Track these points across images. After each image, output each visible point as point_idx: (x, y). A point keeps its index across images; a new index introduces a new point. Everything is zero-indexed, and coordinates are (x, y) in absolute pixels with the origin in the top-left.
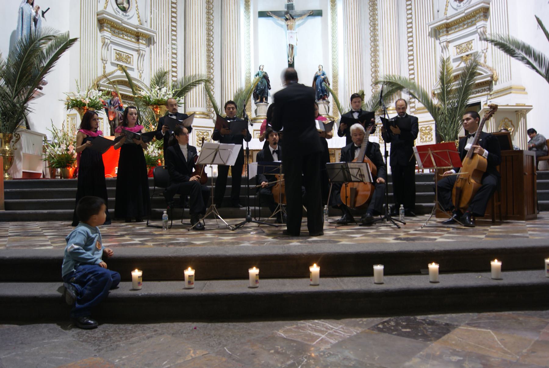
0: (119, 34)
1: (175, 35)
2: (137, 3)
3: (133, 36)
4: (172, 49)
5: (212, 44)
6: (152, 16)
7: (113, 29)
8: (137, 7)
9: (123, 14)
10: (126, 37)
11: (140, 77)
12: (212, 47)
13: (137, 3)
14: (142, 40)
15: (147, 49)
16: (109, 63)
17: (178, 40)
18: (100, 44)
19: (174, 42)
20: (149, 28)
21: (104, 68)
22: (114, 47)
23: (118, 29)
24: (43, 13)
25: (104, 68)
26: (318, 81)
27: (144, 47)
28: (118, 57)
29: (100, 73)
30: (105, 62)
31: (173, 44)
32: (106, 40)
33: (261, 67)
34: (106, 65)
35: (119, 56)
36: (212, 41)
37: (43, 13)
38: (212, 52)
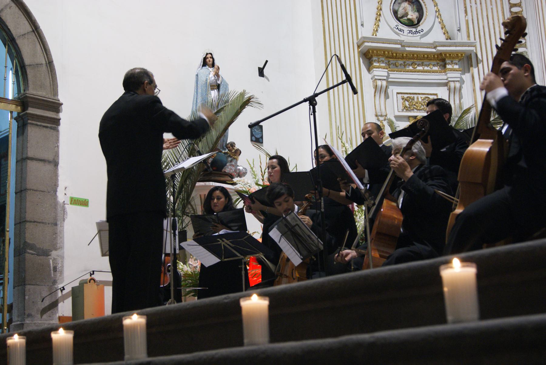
0: (405, 66)
2: (436, 5)
3: (434, 62)
6: (469, 17)
7: (392, 61)
8: (438, 11)
9: (410, 32)
13: (436, 5)
14: (452, 63)
15: (467, 77)
20: (465, 40)
22: (393, 90)
23: (396, 58)
24: (261, 72)
27: (457, 75)
28: (407, 104)
32: (379, 83)
37: (261, 72)
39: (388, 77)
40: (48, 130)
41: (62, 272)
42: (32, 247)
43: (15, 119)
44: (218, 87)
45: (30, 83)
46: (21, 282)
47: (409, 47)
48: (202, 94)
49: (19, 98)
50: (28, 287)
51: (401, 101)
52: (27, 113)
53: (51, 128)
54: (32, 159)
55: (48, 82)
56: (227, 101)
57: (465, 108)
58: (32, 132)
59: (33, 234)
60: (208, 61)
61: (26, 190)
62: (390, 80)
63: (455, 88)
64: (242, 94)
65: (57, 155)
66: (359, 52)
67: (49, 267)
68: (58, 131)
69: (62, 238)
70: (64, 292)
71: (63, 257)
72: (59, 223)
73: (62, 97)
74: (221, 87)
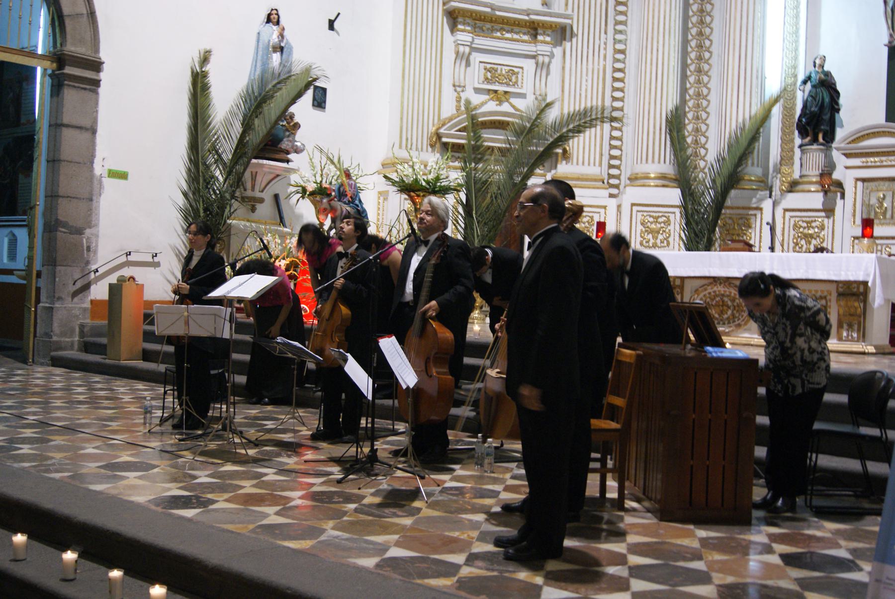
0: (492, 31)
3: (525, 30)
4: (616, 41)
5: (708, 19)
10: (508, 35)
12: (708, 26)
14: (544, 34)
15: (558, 51)
22: (476, 57)
24: (331, 25)
27: (547, 48)
28: (489, 75)
30: (459, 89)
31: (617, 32)
32: (461, 49)
33: (818, 62)
35: (492, 74)
37: (331, 25)
39: (472, 43)
40: (87, 92)
41: (95, 252)
42: (65, 225)
43: (50, 76)
44: (282, 49)
45: (68, 37)
46: (51, 260)
47: (499, 11)
48: (262, 57)
49: (55, 54)
50: (58, 268)
51: (483, 71)
52: (63, 74)
53: (90, 90)
54: (67, 126)
55: (88, 36)
56: (290, 71)
57: (548, 100)
58: (70, 95)
59: (66, 211)
60: (272, 18)
61: (59, 161)
62: (474, 46)
63: (543, 63)
64: (308, 70)
65: (95, 121)
66: (444, 10)
67: (82, 246)
68: (97, 93)
69: (98, 214)
70: (97, 274)
71: (97, 236)
72: (94, 198)
73: (103, 55)
74: (285, 50)
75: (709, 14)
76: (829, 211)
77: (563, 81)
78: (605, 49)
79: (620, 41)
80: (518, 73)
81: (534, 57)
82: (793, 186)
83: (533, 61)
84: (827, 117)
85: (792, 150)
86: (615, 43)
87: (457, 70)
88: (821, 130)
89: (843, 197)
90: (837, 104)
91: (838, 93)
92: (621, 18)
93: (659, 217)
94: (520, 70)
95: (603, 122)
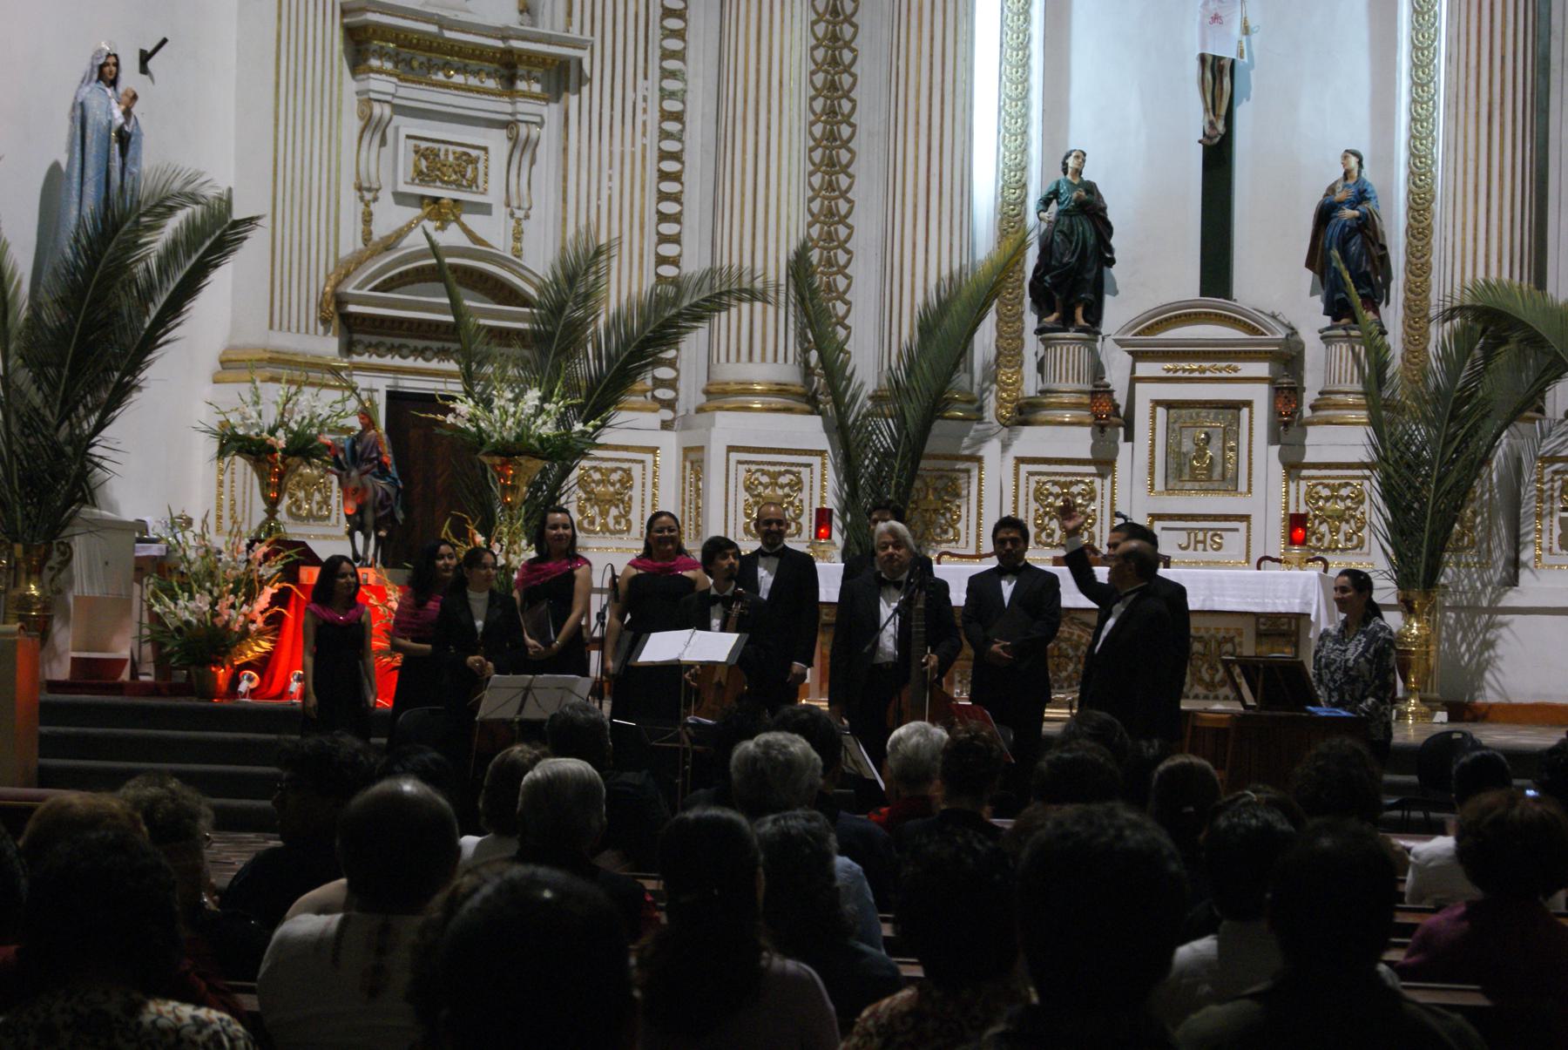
0: (430, 67)
1: (680, 34)
4: (665, 94)
5: (847, 56)
7: (405, 53)
10: (458, 79)
11: (518, 236)
12: (847, 69)
14: (528, 77)
15: (551, 112)
16: (386, 197)
17: (690, 54)
18: (351, 124)
19: (671, 64)
21: (368, 218)
25: (368, 218)
26: (1333, 230)
28: (424, 163)
29: (350, 242)
30: (368, 196)
31: (667, 74)
33: (1071, 162)
34: (374, 207)
35: (430, 163)
36: (848, 45)
38: (847, 95)
47: (451, 29)
75: (848, 45)
76: (1104, 463)
77: (565, 179)
78: (645, 111)
79: (672, 95)
80: (476, 160)
81: (508, 125)
82: (1025, 413)
83: (504, 132)
84: (1090, 276)
85: (1019, 335)
86: (662, 98)
87: (364, 154)
88: (1080, 301)
89: (1129, 437)
90: (1110, 250)
91: (1108, 228)
92: (673, 44)
93: (780, 474)
94: (481, 153)
95: (740, 300)
